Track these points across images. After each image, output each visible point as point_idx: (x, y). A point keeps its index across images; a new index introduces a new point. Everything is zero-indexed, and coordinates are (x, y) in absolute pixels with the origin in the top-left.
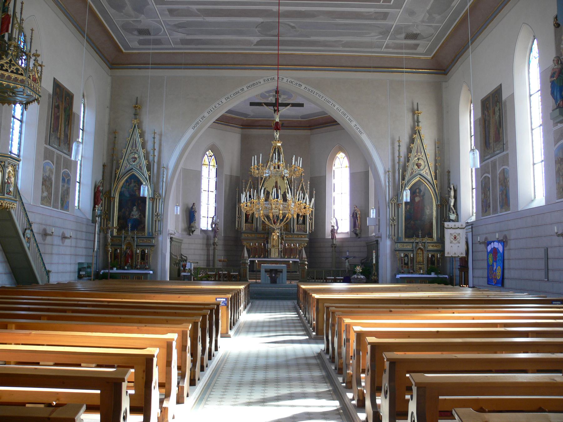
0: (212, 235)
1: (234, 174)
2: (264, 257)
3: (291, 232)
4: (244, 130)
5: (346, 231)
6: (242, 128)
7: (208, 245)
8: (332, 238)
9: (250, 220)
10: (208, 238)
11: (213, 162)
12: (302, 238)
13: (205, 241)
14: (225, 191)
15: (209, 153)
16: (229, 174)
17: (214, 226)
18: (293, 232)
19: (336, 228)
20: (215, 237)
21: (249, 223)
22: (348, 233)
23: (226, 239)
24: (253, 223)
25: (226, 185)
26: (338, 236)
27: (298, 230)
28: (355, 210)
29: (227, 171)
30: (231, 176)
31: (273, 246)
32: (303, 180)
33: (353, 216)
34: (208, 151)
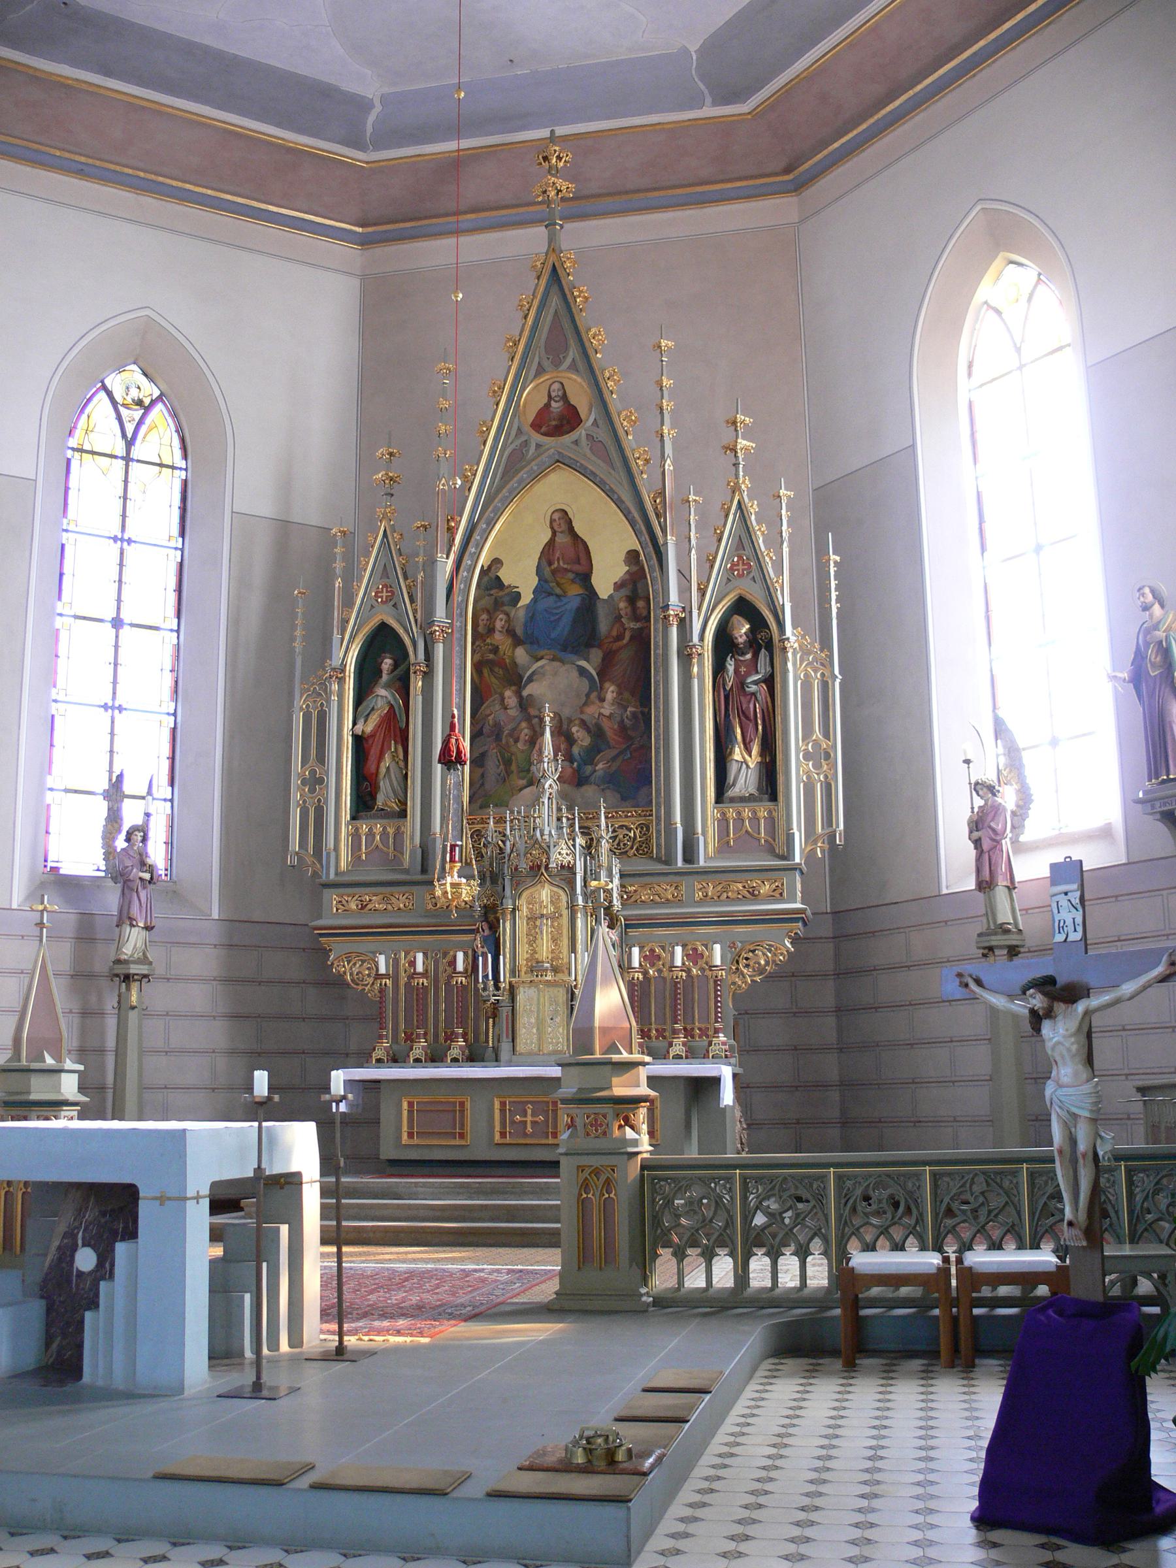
0: (111, 900)
1: (310, 511)
2: (473, 1057)
3: (669, 860)
4: (379, 251)
5: (1097, 823)
6: (365, 242)
7: (82, 977)
8: (985, 885)
9: (384, 797)
10: (86, 934)
11: (160, 438)
12: (753, 895)
13: (62, 956)
14: (235, 622)
15: (129, 382)
16: (265, 507)
17: (120, 843)
18: (690, 854)
19: (1008, 798)
20: (125, 918)
21: (385, 814)
22: (1105, 833)
23: (243, 937)
24: (403, 814)
25: (241, 583)
26: (1030, 868)
27: (724, 847)
28: (1148, 630)
29: (250, 489)
30: (284, 528)
31: (535, 967)
32: (745, 483)
33: (1137, 678)
34: (120, 369)
